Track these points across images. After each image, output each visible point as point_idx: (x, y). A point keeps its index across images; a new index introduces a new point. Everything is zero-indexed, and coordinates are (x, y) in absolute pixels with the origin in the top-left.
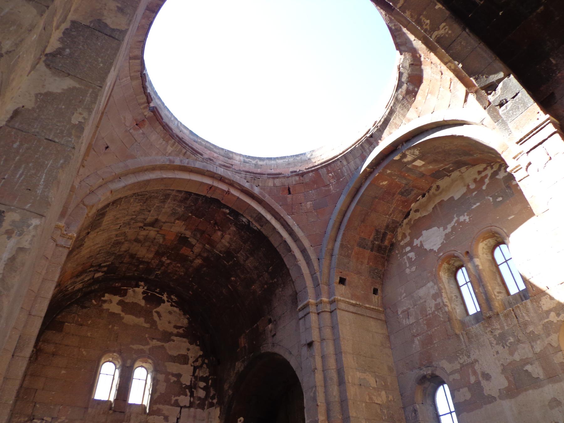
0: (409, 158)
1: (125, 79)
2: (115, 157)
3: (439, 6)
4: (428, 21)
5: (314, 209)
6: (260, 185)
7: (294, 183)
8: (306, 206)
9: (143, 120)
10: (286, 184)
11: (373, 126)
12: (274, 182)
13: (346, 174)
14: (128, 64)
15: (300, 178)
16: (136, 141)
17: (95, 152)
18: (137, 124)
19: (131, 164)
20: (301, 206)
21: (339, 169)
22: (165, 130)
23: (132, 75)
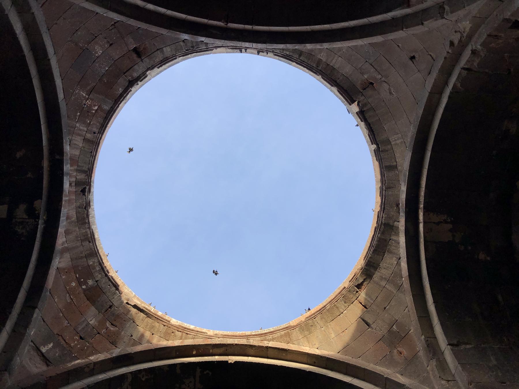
0: (21, 212)
1: (398, 142)
2: (400, 45)
4: (143, 379)
5: (88, 49)
6: (182, 43)
7: (136, 67)
8: (101, 46)
9: (364, 89)
10: (146, 60)
11: (89, 200)
12: (163, 54)
13: (77, 125)
14: (397, 160)
15: (132, 77)
16: (371, 65)
17: (431, 55)
18: (372, 84)
19: (378, 39)
20: (108, 42)
21: (90, 122)
22: (334, 80)
23: (389, 147)
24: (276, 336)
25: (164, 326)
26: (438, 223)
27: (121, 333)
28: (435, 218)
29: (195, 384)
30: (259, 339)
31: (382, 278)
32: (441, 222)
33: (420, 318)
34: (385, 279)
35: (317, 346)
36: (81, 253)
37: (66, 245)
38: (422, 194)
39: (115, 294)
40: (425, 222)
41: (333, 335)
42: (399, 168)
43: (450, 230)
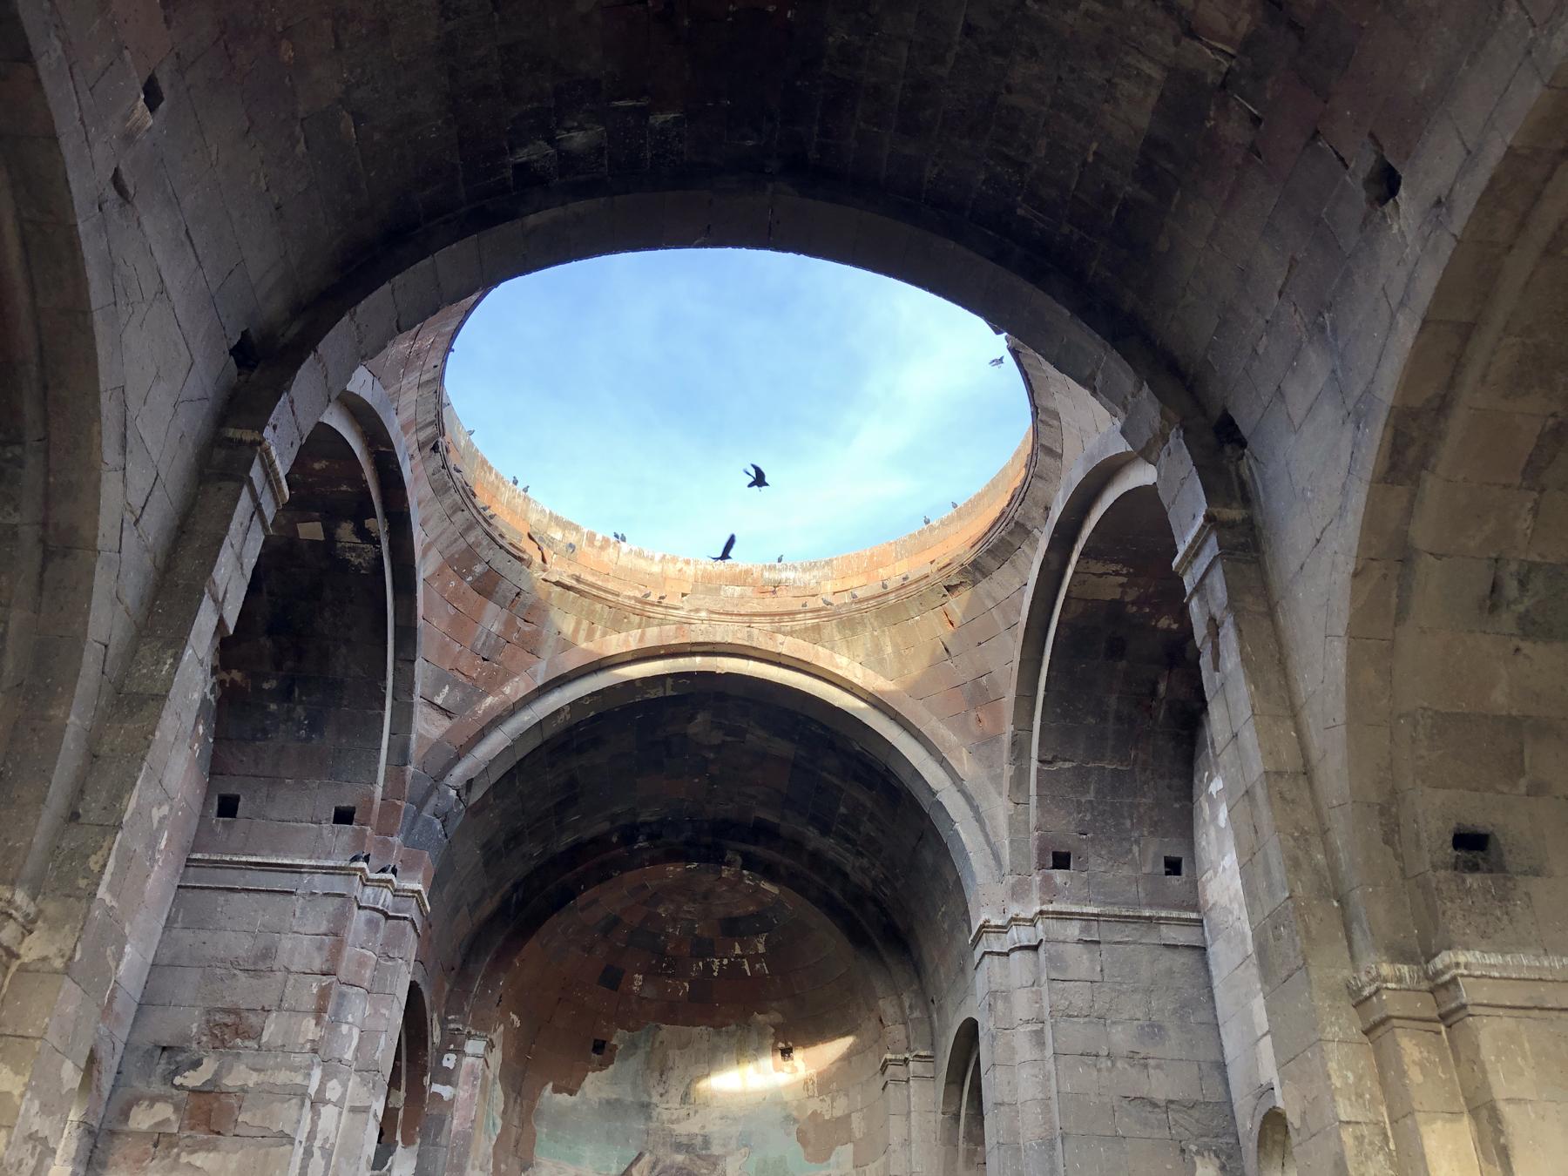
0: (346, 532)
3: (592, 714)
23: (1055, 423)
24: (798, 628)
25: (610, 607)
26: (1101, 575)
27: (541, 632)
28: (1097, 567)
29: (665, 693)
30: (768, 627)
31: (989, 595)
32: (1108, 574)
33: (1019, 697)
34: (994, 599)
35: (861, 659)
36: (454, 534)
37: (428, 540)
38: (1086, 532)
39: (521, 572)
40: (1075, 572)
41: (889, 650)
42: (1065, 462)
43: (1122, 585)
